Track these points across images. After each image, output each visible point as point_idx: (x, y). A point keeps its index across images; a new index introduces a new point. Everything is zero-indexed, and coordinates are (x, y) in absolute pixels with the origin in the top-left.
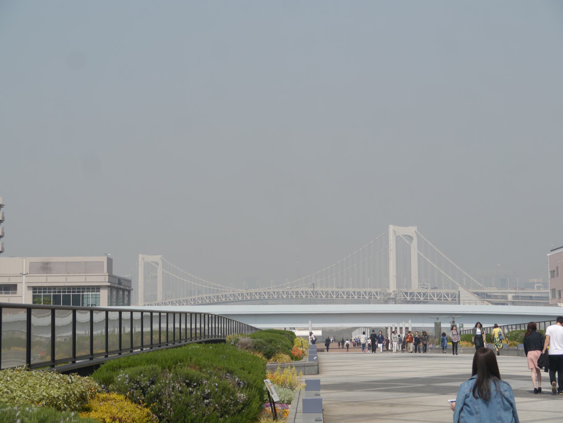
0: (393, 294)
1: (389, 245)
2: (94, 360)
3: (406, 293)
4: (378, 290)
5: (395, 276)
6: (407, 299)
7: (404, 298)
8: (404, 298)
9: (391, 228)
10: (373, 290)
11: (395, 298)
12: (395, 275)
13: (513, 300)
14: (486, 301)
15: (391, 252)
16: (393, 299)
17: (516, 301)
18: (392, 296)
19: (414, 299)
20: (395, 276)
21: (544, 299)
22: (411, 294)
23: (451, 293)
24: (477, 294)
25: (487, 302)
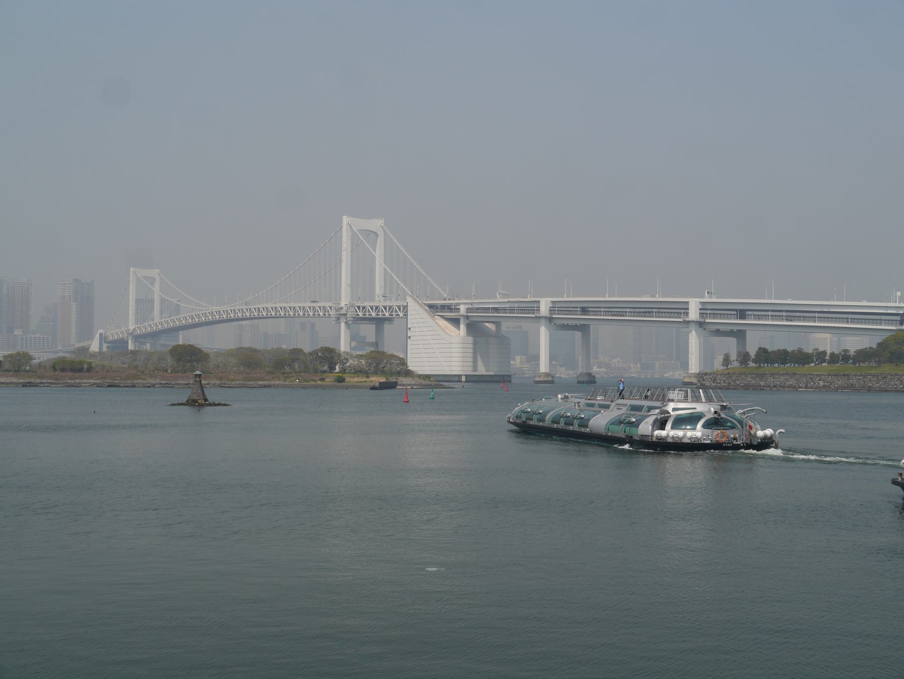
0: (345, 308)
1: (343, 242)
2: (398, 388)
3: (359, 307)
4: (331, 304)
5: (349, 285)
6: (358, 315)
7: (356, 313)
8: (356, 313)
9: (345, 219)
10: (327, 305)
11: (346, 314)
12: (349, 283)
13: (465, 314)
14: (438, 315)
15: (345, 251)
16: (346, 315)
17: (469, 314)
18: (343, 312)
19: (366, 315)
20: (349, 285)
21: (522, 311)
22: (364, 308)
23: (402, 305)
24: (431, 307)
25: (439, 317)
